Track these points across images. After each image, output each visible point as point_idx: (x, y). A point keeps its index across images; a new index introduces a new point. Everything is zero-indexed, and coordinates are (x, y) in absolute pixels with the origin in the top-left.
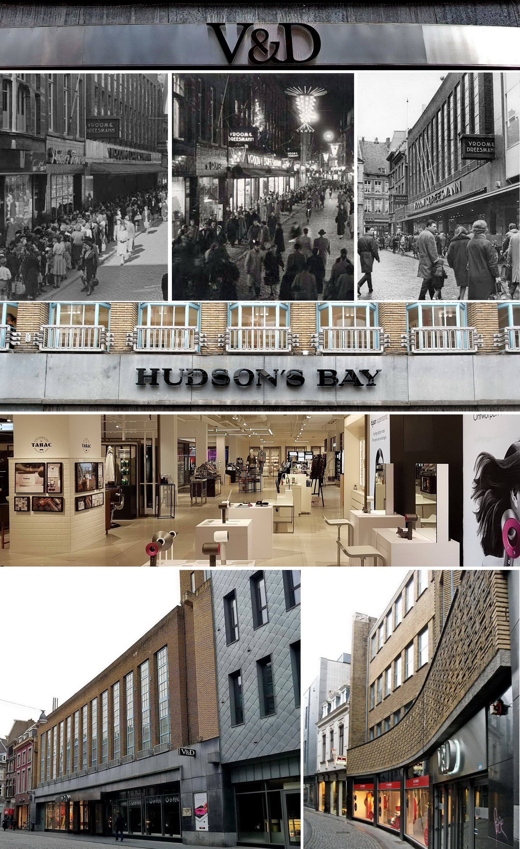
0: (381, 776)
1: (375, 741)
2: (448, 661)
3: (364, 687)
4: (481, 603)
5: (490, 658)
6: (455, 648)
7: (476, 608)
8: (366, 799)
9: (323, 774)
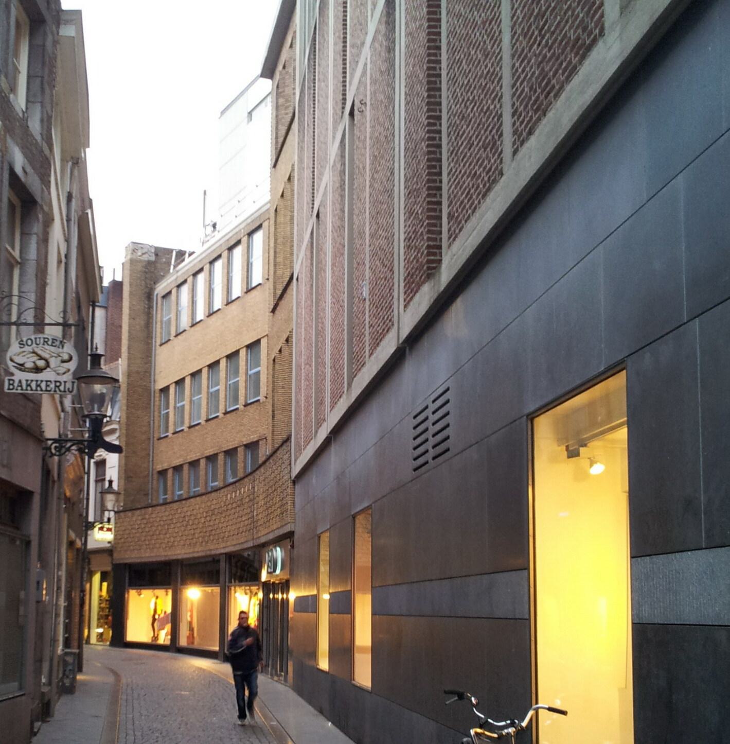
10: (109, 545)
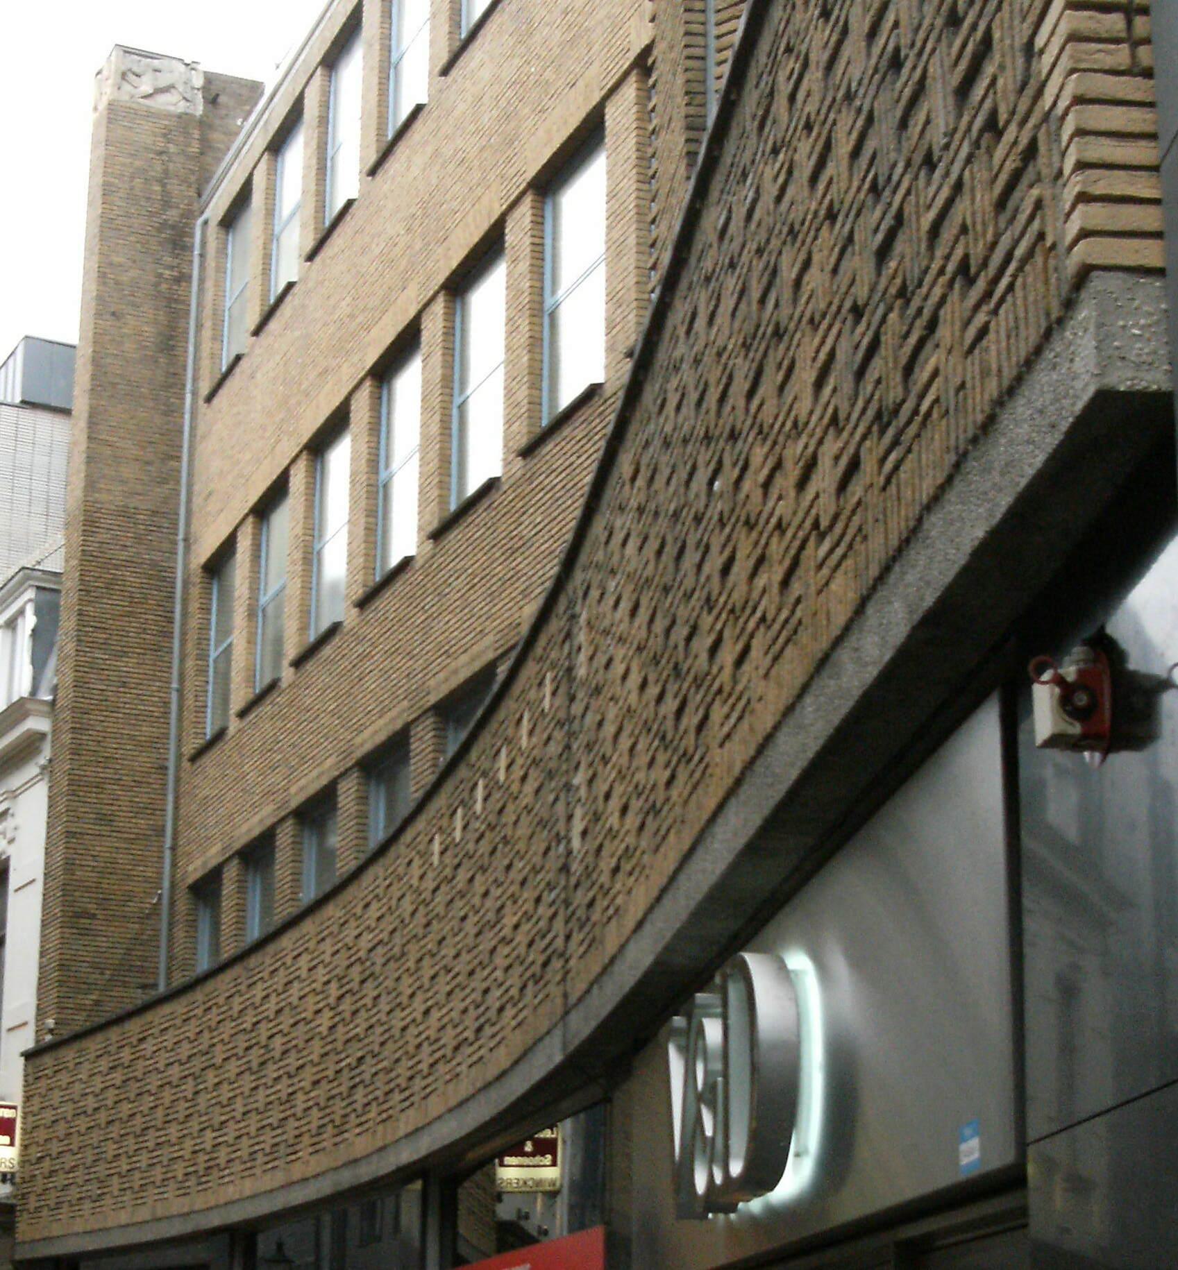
0: (265, 1245)
2: (743, 370)
3: (161, 577)
5: (1031, 336)
6: (788, 273)
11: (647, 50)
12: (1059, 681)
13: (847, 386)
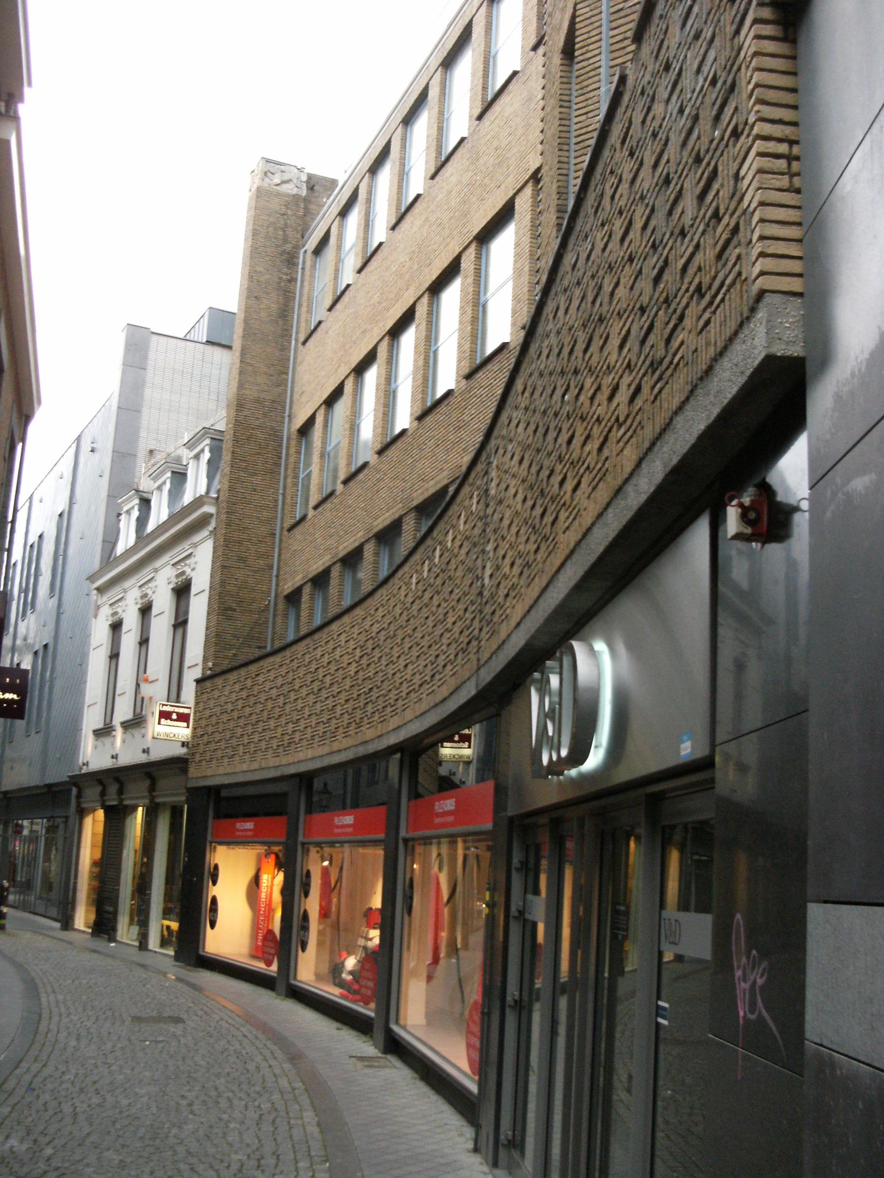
0: (317, 784)
1: (301, 647)
2: (582, 338)
3: (276, 435)
4: (705, 124)
5: (733, 325)
6: (607, 288)
7: (684, 144)
8: (256, 880)
9: (102, 778)
10: (184, 750)
11: (538, 170)
12: (741, 505)
13: (636, 348)
